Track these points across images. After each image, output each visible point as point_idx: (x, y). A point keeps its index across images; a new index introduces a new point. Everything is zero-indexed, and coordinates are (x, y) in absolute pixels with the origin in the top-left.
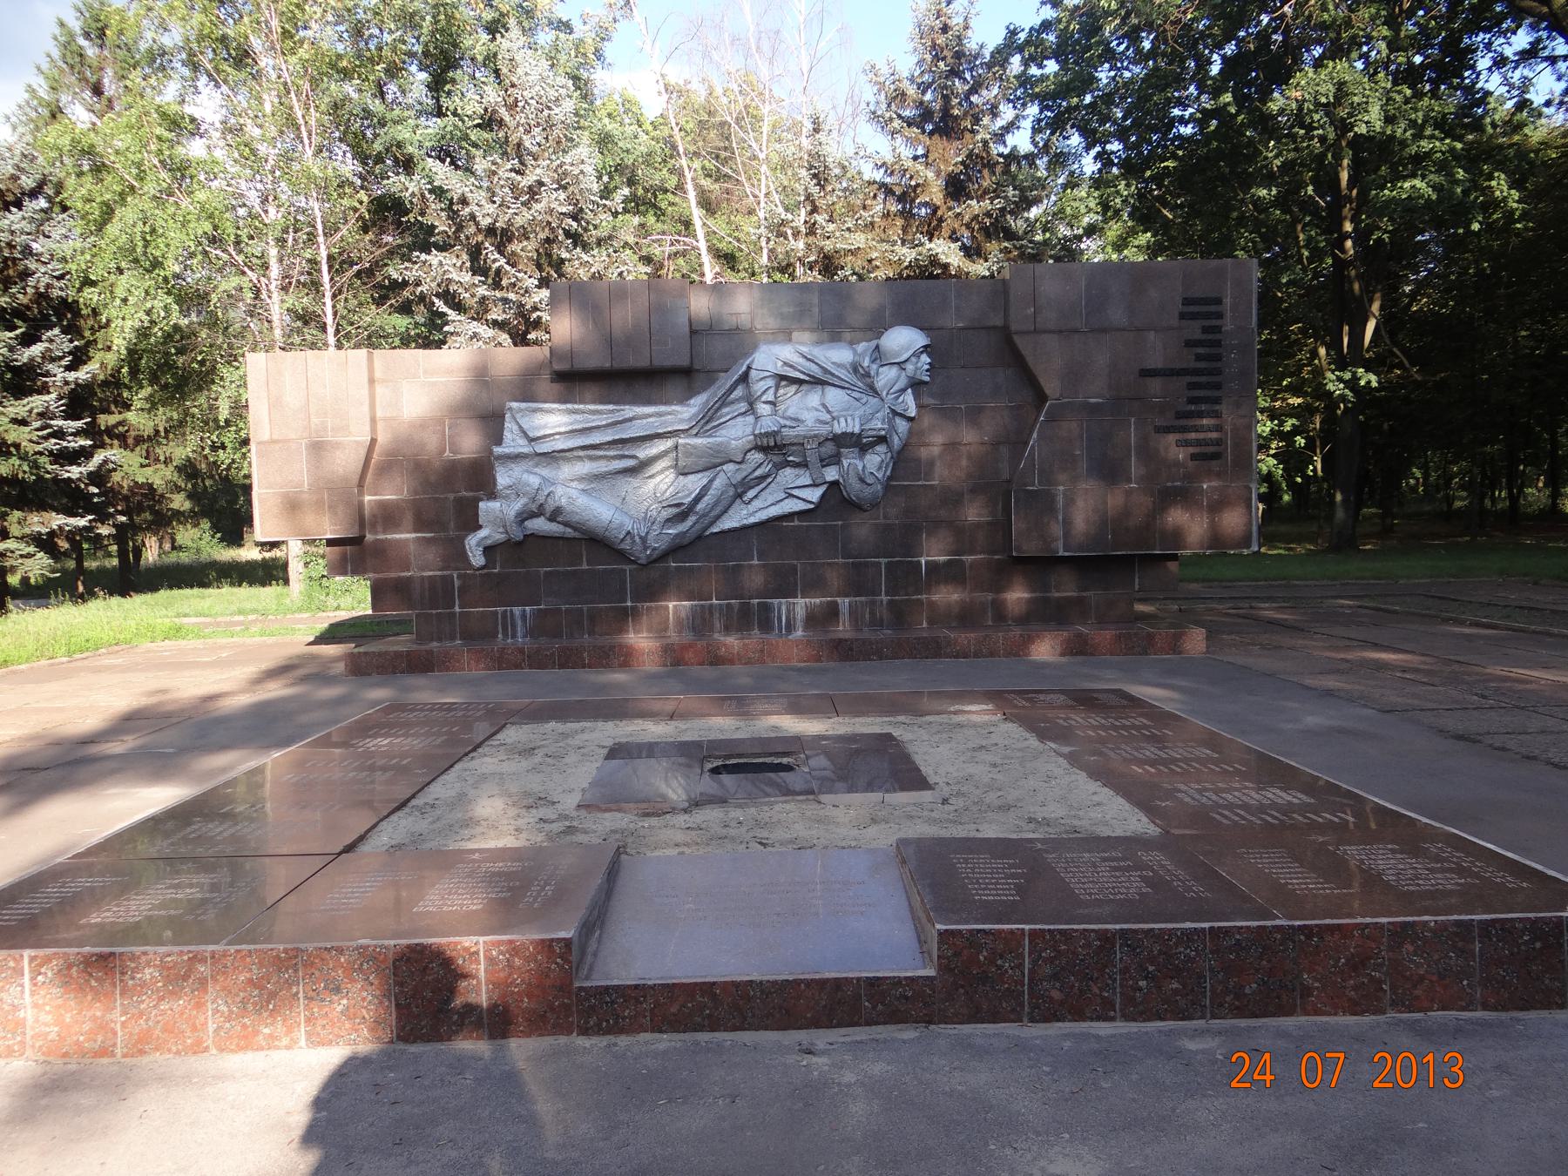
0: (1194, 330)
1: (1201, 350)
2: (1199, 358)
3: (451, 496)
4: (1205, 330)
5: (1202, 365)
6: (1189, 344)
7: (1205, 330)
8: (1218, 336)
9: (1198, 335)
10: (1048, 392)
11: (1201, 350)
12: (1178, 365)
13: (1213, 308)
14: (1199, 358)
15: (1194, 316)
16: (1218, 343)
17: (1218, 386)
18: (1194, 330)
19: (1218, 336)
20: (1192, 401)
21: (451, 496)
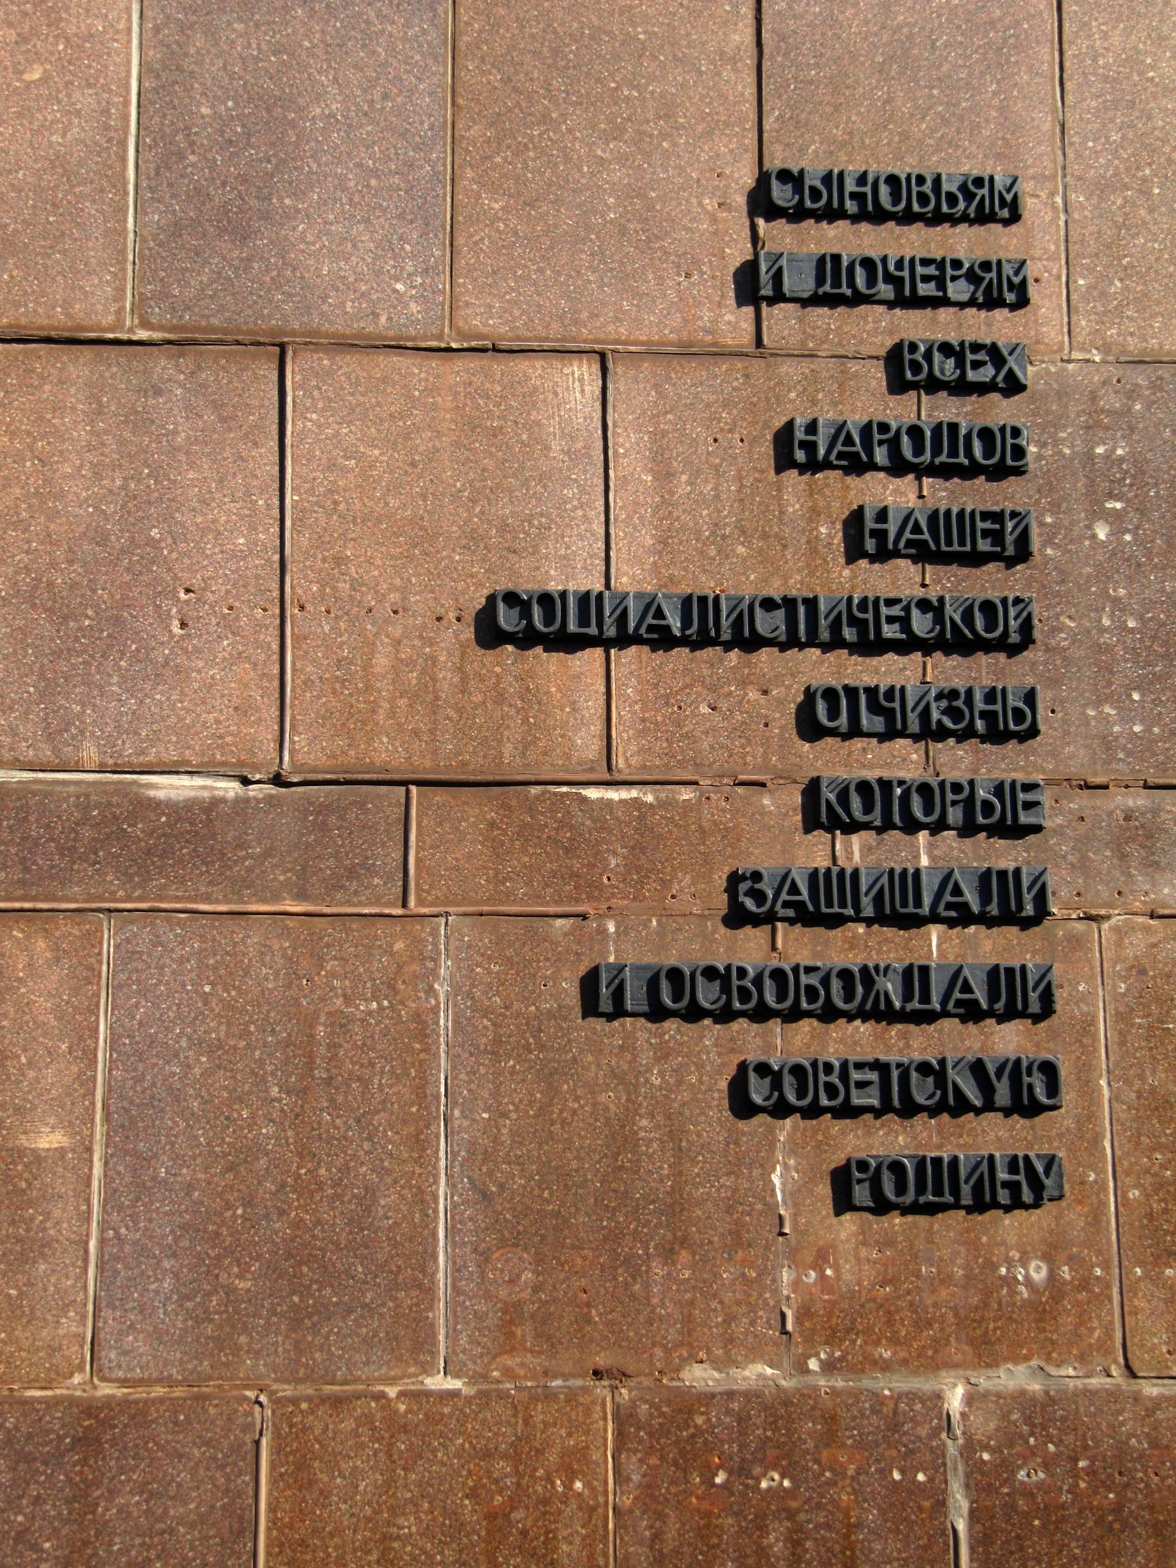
0: (838, 368)
1: (897, 495)
4: (903, 369)
5: (902, 579)
6: (792, 450)
7: (903, 369)
8: (1000, 411)
9: (868, 401)
11: (897, 495)
12: (735, 577)
13: (964, 243)
14: (864, 538)
15: (836, 286)
16: (1002, 458)
17: (1011, 723)
18: (838, 368)
19: (1000, 411)
20: (822, 811)
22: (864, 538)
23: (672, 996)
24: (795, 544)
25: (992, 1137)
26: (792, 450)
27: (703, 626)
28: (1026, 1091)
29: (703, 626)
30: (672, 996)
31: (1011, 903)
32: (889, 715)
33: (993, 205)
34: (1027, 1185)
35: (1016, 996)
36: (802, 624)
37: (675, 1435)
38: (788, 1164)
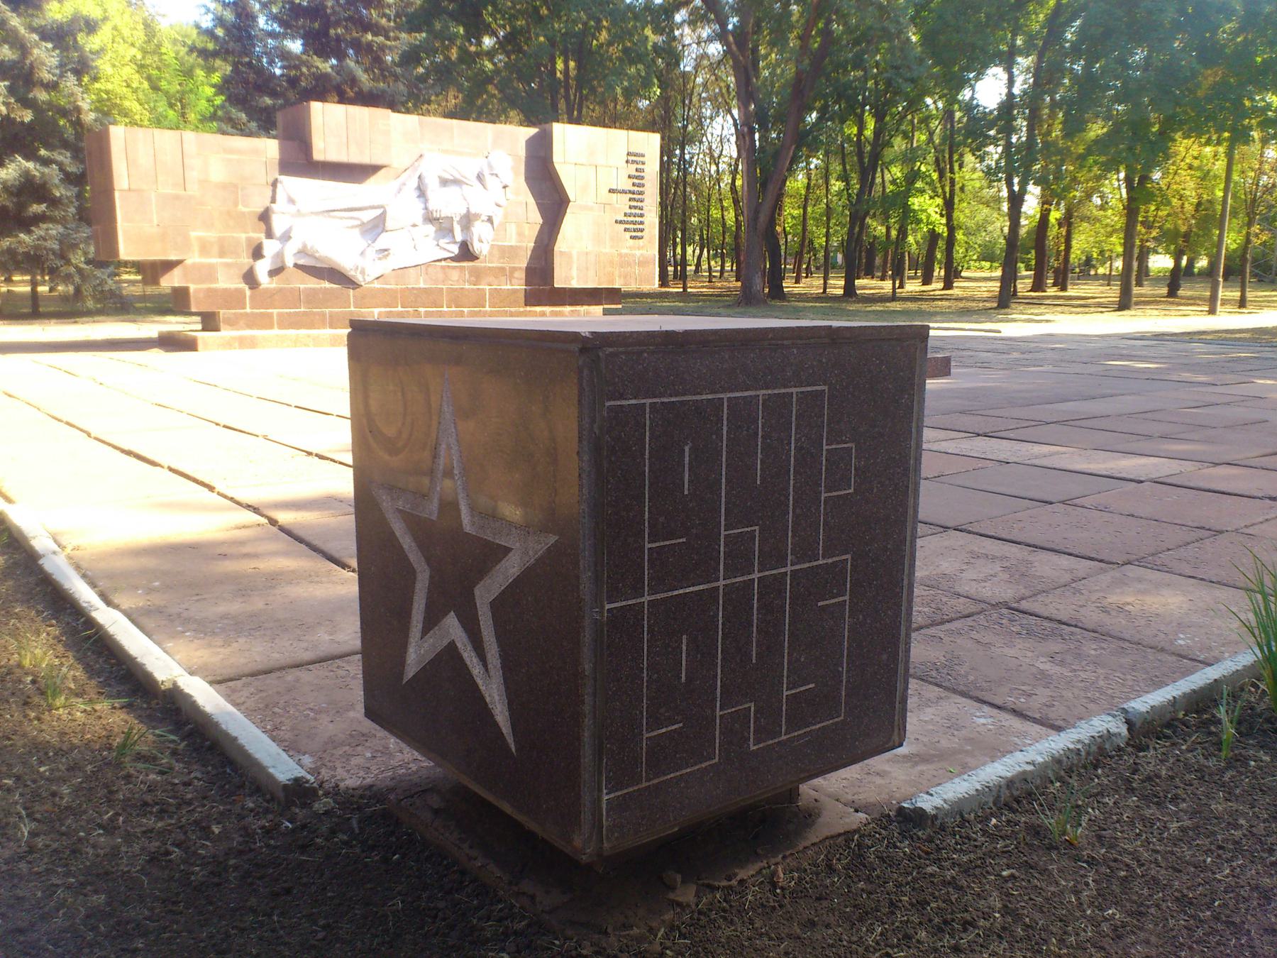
0: (632, 169)
2: (634, 185)
3: (243, 236)
5: (636, 189)
9: (634, 173)
10: (571, 197)
15: (633, 162)
21: (243, 236)
22: (634, 185)
23: (621, 222)
24: (626, 184)
25: (639, 234)
26: (630, 177)
27: (624, 192)
28: (642, 230)
29: (624, 192)
30: (621, 222)
31: (642, 216)
32: (634, 199)
33: (643, 156)
34: (642, 238)
35: (642, 223)
36: (630, 192)
37: (620, 255)
38: (628, 234)
